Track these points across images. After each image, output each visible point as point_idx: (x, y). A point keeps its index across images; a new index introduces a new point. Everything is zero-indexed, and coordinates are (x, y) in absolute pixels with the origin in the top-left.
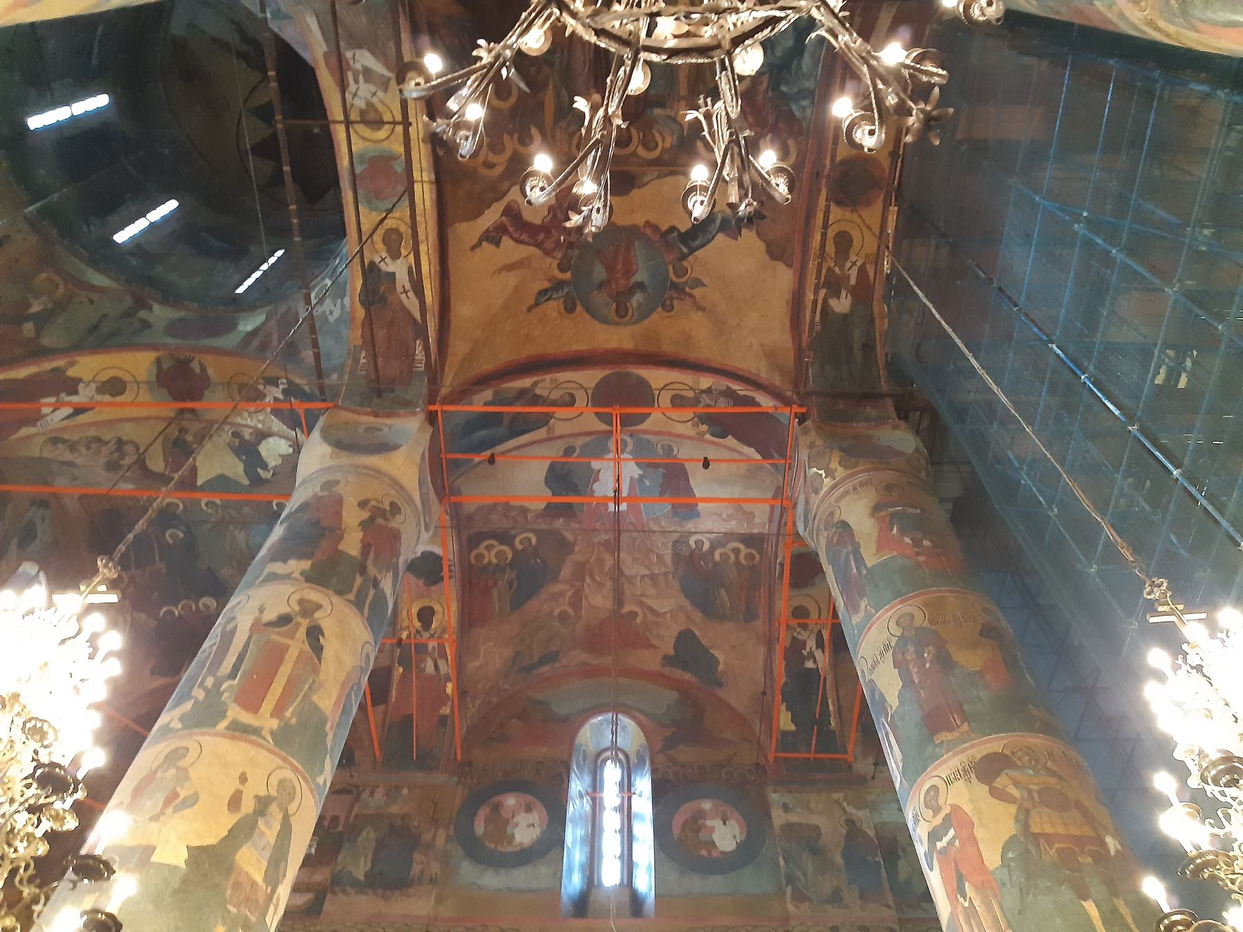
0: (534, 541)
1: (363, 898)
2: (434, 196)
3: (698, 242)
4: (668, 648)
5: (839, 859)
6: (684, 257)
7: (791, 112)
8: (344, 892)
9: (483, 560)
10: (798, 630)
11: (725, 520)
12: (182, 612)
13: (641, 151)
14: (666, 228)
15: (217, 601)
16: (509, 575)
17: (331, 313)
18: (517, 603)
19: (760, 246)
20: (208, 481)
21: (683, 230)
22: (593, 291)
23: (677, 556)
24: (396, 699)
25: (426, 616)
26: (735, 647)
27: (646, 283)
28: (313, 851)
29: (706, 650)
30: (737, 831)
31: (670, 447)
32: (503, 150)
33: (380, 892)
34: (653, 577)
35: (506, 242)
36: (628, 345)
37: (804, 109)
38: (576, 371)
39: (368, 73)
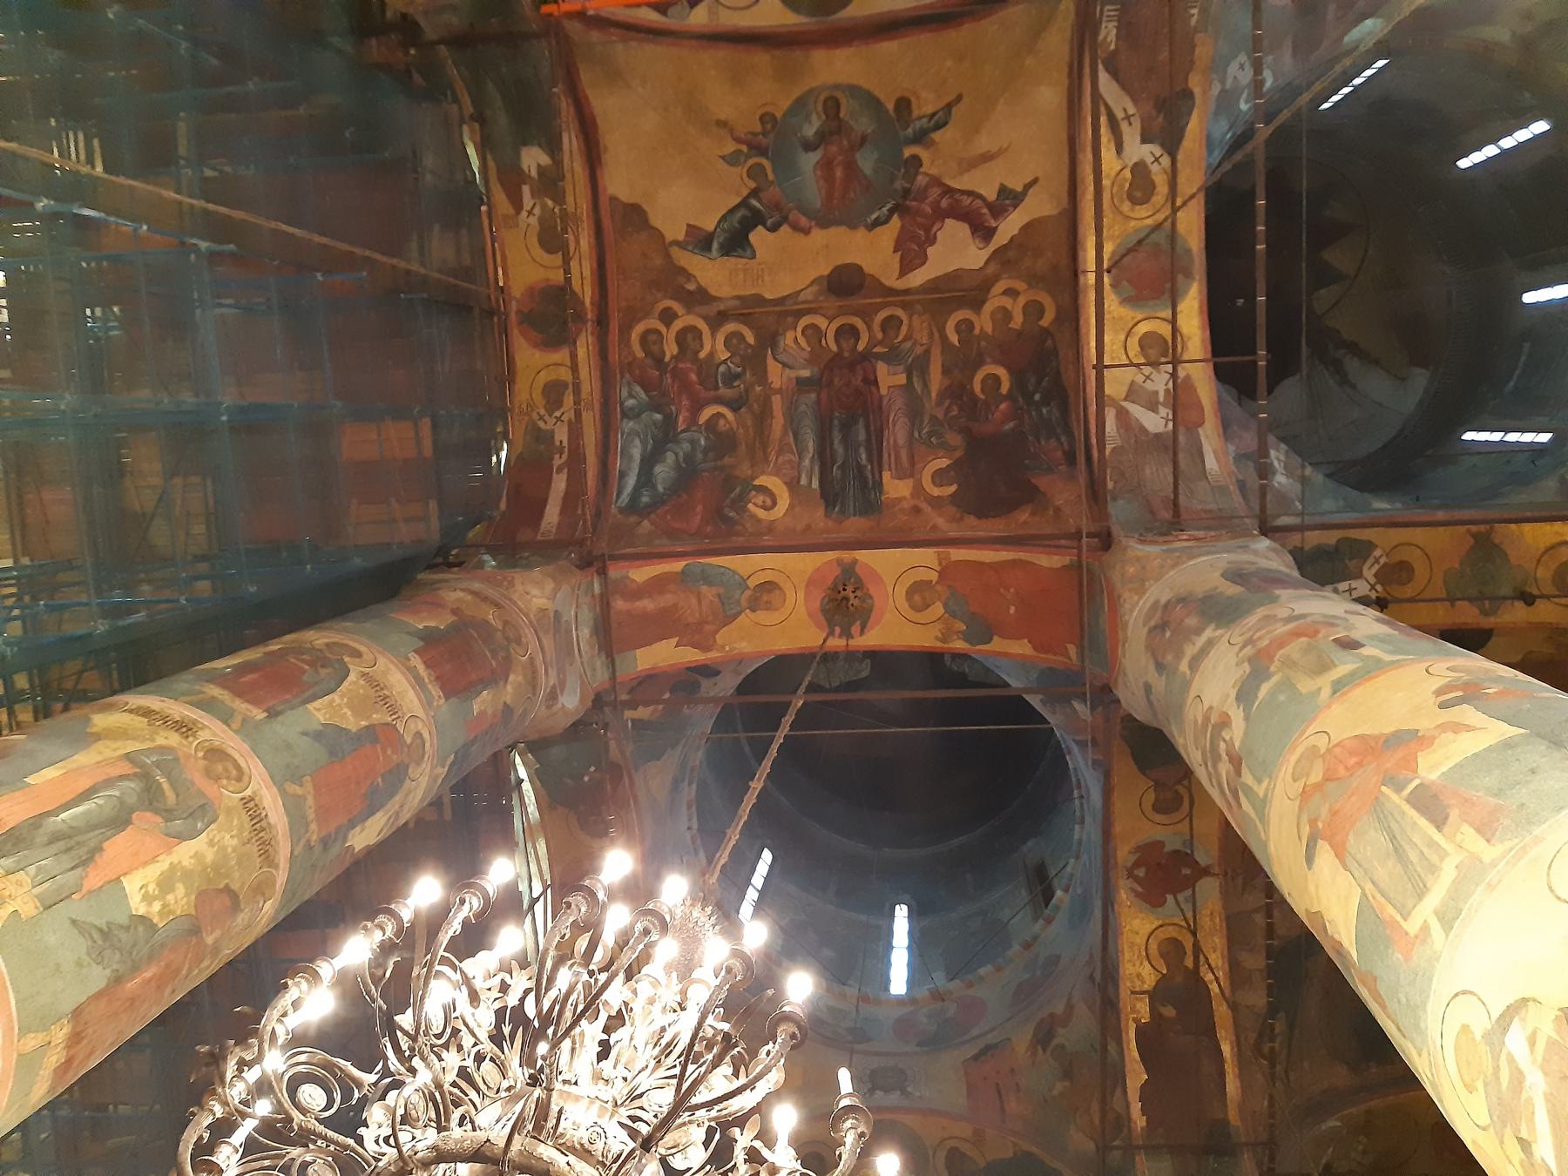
2: (1080, 253)
3: (739, 215)
6: (754, 193)
7: (646, 391)
13: (822, 322)
14: (782, 228)
17: (1242, 67)
19: (656, 220)
21: (760, 228)
22: (873, 131)
27: (800, 149)
32: (993, 313)
35: (991, 195)
36: (819, 56)
37: (631, 396)
38: (889, 12)
39: (1152, 406)
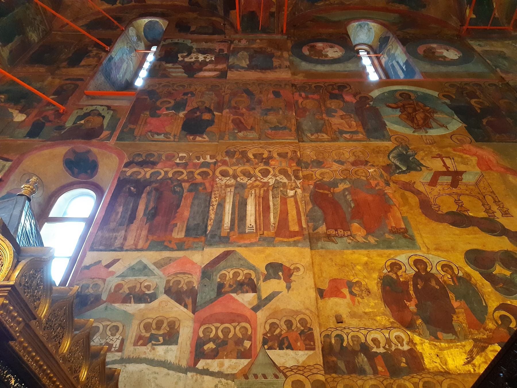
1: (249, 72)
30: (456, 53)
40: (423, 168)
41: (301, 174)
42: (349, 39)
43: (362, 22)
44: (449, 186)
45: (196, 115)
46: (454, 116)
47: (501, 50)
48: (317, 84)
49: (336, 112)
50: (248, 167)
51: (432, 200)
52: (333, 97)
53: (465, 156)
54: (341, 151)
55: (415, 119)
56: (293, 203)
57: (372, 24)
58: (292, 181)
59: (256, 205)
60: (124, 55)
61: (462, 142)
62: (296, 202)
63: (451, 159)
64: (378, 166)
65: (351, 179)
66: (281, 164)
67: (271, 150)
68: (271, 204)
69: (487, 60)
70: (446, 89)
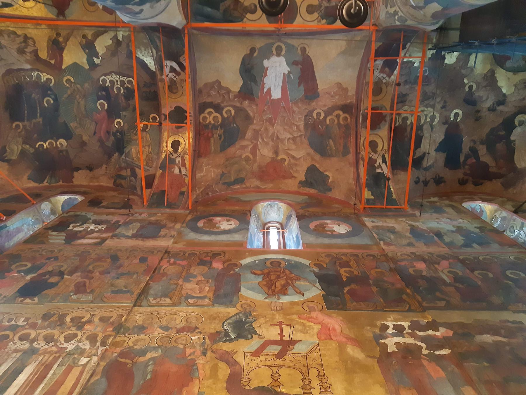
0: (233, 114)
1: (130, 240)
4: (301, 177)
5: (408, 234)
8: (119, 239)
9: (207, 121)
10: (372, 154)
11: (332, 96)
12: (48, 147)
15: (66, 140)
16: (220, 131)
18: (223, 148)
20: (68, 67)
23: (306, 125)
24: (157, 184)
25: (176, 145)
26: (338, 170)
28: (103, 229)
29: (321, 173)
31: (304, 48)
33: (140, 239)
34: (294, 139)
40: (254, 336)
41: (110, 341)
42: (249, 215)
43: (272, 202)
44: (274, 357)
45: (44, 278)
46: (316, 283)
47: (392, 225)
48: (193, 252)
49: (195, 277)
50: (56, 332)
51: (245, 373)
52: (202, 263)
53: (308, 324)
54: (175, 316)
55: (274, 285)
56: (78, 373)
57: (281, 204)
58: (95, 348)
59: (31, 374)
60: (25, 225)
61: (312, 309)
62: (81, 373)
63: (291, 327)
64: (205, 333)
65: (166, 347)
66: (95, 329)
67: (96, 313)
68: (51, 372)
69: (375, 235)
70: (321, 259)
